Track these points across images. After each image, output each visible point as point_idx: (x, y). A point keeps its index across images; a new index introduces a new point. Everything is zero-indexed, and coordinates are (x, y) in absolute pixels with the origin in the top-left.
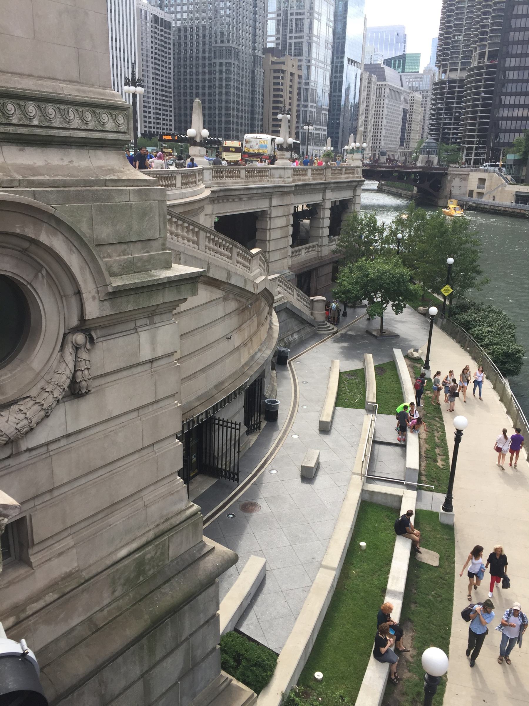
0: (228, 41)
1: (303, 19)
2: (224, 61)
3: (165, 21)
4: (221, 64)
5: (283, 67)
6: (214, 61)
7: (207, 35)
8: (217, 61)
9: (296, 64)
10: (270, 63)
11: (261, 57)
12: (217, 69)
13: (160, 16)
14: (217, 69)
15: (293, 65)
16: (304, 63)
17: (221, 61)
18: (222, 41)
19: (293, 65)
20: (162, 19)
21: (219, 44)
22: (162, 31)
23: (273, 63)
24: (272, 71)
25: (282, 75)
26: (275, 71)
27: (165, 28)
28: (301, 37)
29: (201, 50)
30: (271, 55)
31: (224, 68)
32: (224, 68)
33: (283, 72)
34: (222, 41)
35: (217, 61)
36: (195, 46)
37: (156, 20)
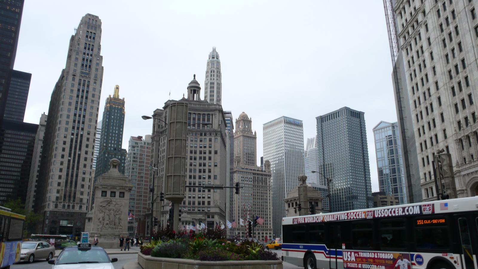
0: (352, 193)
1: (396, 178)
2: (351, 201)
3: (325, 189)
4: (350, 203)
5: (385, 200)
6: (347, 202)
7: (348, 191)
8: (348, 202)
9: (393, 198)
10: (379, 198)
11: (371, 197)
12: (349, 205)
13: (322, 188)
14: (349, 205)
15: (391, 198)
16: (399, 196)
17: (350, 201)
18: (350, 194)
19: (391, 198)
20: (323, 189)
21: (349, 195)
22: (323, 193)
23: (381, 198)
24: (380, 202)
25: (385, 203)
26: (382, 202)
27: (325, 191)
28: (397, 185)
29: (337, 198)
30: (379, 195)
31: (351, 204)
32: (351, 204)
33: (386, 202)
34: (350, 194)
35: (348, 202)
36: (337, 197)
37: (320, 189)
